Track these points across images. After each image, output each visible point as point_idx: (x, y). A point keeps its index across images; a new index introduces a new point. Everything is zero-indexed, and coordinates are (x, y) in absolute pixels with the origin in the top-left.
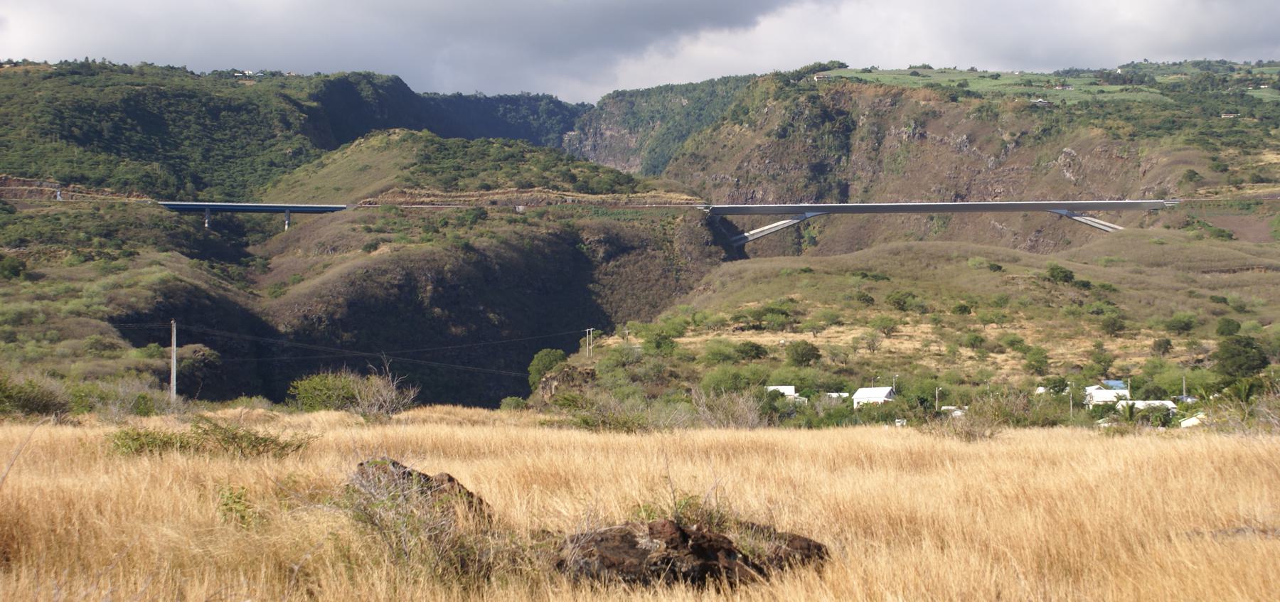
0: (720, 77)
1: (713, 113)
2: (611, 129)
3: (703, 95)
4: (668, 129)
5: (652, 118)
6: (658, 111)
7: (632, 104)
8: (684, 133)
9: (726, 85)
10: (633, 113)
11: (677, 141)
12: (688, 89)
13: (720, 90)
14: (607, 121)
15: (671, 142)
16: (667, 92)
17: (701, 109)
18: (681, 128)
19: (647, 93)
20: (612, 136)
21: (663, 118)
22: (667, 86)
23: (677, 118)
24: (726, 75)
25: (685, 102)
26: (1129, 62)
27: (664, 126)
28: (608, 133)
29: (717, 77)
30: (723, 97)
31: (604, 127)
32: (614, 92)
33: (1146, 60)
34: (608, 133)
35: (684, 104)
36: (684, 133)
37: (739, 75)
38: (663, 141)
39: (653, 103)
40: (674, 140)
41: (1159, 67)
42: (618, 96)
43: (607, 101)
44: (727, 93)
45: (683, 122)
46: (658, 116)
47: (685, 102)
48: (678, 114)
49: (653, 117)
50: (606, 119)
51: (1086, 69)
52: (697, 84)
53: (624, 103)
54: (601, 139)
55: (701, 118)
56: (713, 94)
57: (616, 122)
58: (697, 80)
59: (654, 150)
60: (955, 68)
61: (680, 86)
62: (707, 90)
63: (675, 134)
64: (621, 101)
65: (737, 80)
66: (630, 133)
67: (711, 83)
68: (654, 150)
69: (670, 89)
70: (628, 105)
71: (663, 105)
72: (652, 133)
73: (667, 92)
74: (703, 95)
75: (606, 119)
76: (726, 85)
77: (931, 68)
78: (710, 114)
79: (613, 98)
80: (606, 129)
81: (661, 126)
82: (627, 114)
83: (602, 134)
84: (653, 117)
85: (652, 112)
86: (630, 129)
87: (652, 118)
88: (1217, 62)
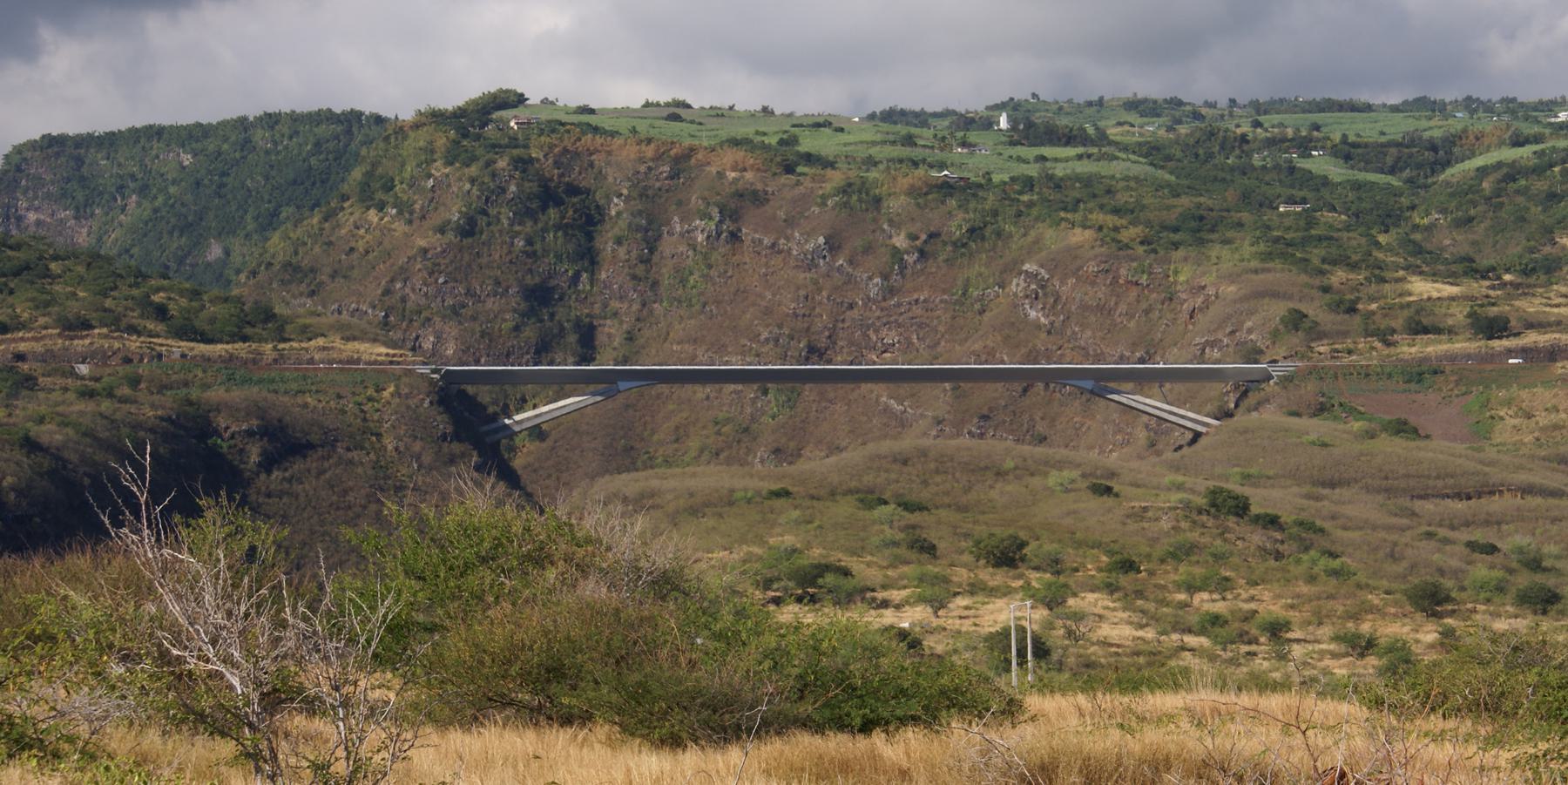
0: (260, 113)
1: (249, 183)
2: (37, 210)
3: (225, 147)
4: (156, 211)
5: (121, 188)
6: (133, 177)
7: (80, 161)
8: (190, 218)
9: (272, 128)
10: (83, 179)
11: (176, 234)
12: (194, 135)
13: (260, 137)
14: (31, 193)
15: (165, 236)
16: (150, 139)
17: (224, 174)
18: (184, 210)
19: (110, 141)
20: (39, 223)
21: (143, 191)
22: (151, 127)
23: (172, 190)
24: (272, 109)
25: (187, 159)
26: (1006, 99)
27: (146, 204)
28: (32, 217)
29: (252, 111)
30: (267, 152)
31: (22, 204)
32: (44, 137)
33: (1034, 95)
34: (32, 217)
35: (186, 163)
36: (190, 218)
37: (298, 111)
38: (145, 235)
39: (122, 160)
40: (171, 233)
41: (1061, 108)
42: (50, 146)
43: (29, 155)
44: (275, 143)
45: (189, 198)
46: (132, 185)
47: (187, 159)
48: (174, 182)
49: (122, 187)
50: (27, 189)
51: (939, 109)
52: (210, 125)
53: (63, 159)
54: (18, 226)
55: (223, 191)
56: (246, 144)
57: (48, 196)
58: (210, 114)
59: (127, 251)
60: (731, 108)
61: (179, 128)
62: (233, 138)
63: (173, 220)
64: (58, 155)
65: (295, 120)
66: (76, 218)
67: (242, 123)
68: (127, 251)
69: (155, 133)
70: (72, 163)
71: (142, 165)
72: (122, 217)
73: (150, 139)
74: (225, 147)
75: (27, 189)
76: (272, 128)
77: (689, 106)
78: (243, 184)
79: (42, 149)
80: (28, 209)
81: (139, 204)
82: (69, 180)
83: (19, 219)
84: (122, 187)
85: (121, 177)
86: (77, 209)
87: (121, 188)
88: (1165, 101)
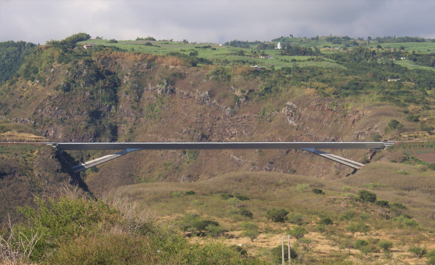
26: (280, 37)
33: (291, 36)
41: (301, 41)
60: (171, 41)
77: (154, 40)
88: (343, 37)
